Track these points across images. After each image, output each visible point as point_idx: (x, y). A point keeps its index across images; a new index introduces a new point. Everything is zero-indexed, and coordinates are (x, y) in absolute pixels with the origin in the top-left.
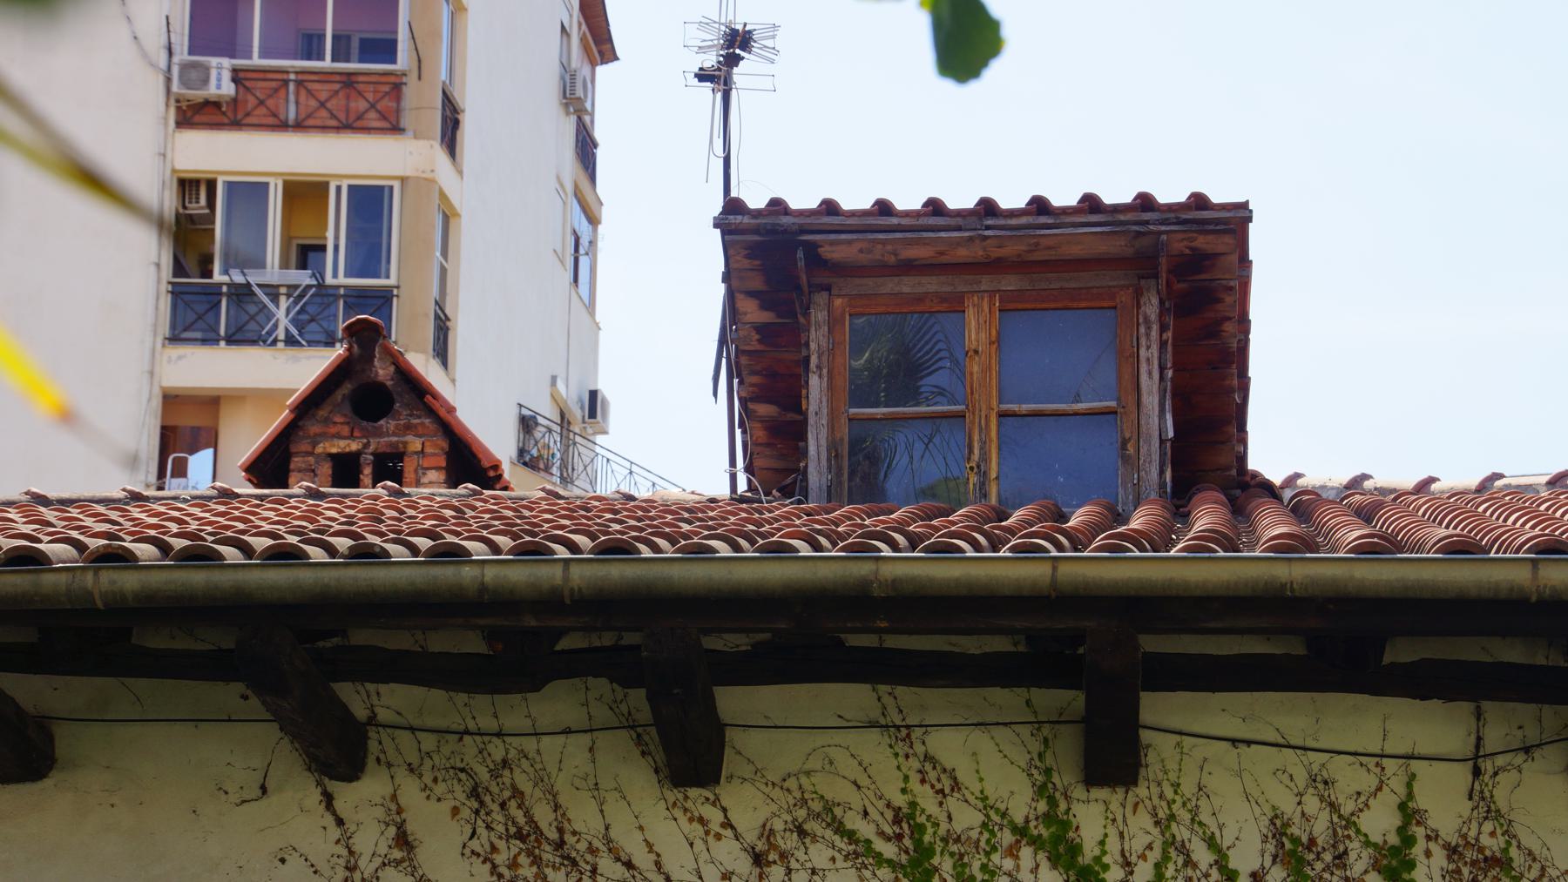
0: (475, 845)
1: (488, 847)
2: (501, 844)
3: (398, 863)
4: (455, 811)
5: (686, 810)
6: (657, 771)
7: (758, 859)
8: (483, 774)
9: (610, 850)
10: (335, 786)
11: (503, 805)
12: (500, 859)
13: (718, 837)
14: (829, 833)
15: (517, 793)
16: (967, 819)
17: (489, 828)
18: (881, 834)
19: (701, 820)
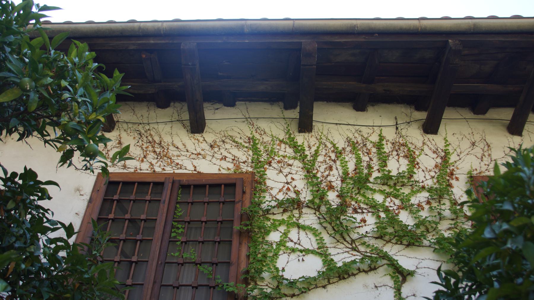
0: (138, 144)
1: (141, 145)
2: (145, 144)
3: (117, 147)
4: (134, 138)
5: (194, 138)
6: (187, 131)
7: (212, 146)
8: (143, 132)
9: (173, 145)
11: (147, 137)
12: (143, 147)
13: (202, 143)
14: (231, 142)
15: (151, 135)
16: (267, 139)
17: (142, 141)
18: (245, 142)
19: (197, 140)
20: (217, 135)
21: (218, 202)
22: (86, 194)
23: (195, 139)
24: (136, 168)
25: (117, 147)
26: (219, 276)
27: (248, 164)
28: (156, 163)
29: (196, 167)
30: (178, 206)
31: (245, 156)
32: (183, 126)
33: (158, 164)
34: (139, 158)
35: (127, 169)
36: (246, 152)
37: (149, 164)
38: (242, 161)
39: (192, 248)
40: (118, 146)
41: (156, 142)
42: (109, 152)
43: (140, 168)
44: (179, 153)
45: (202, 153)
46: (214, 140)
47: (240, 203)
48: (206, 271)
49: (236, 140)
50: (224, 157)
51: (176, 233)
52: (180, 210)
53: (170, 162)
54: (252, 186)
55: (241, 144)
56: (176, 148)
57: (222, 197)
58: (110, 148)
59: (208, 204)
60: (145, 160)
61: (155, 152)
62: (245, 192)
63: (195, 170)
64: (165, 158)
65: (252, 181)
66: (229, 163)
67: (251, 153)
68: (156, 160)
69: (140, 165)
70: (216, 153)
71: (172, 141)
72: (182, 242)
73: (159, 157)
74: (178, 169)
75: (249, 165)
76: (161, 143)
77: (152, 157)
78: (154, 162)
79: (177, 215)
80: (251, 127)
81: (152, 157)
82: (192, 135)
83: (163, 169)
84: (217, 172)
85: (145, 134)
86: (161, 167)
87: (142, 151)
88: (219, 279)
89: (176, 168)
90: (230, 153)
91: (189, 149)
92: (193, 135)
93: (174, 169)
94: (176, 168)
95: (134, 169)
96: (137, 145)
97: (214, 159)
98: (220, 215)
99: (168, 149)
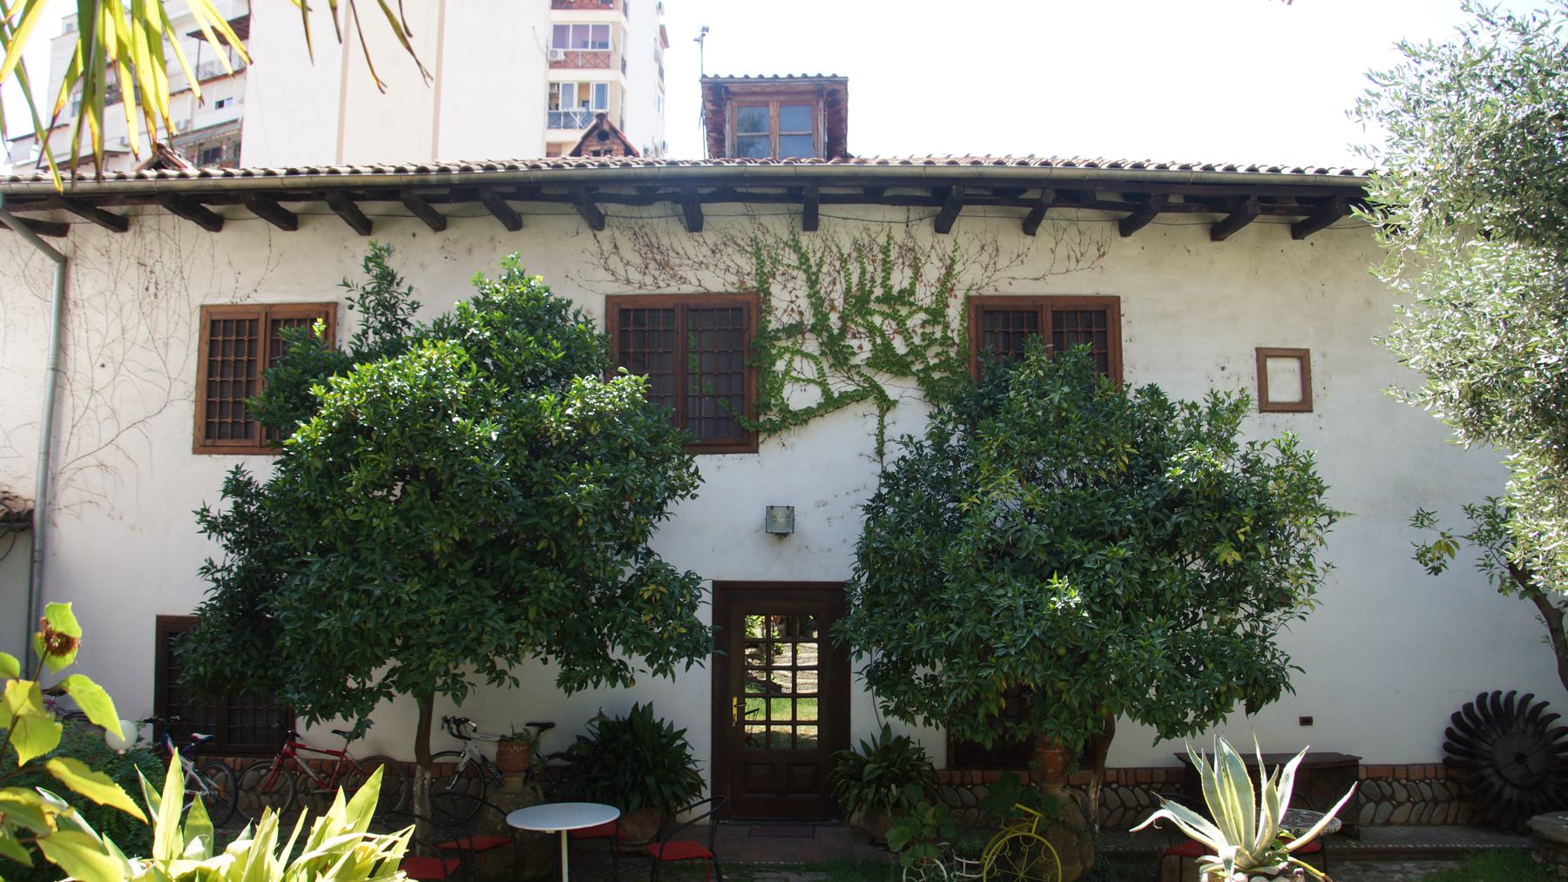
7: (713, 252)
10: (597, 232)
16: (771, 240)
45: (705, 261)
61: (655, 260)
67: (754, 261)
78: (657, 274)
84: (722, 290)
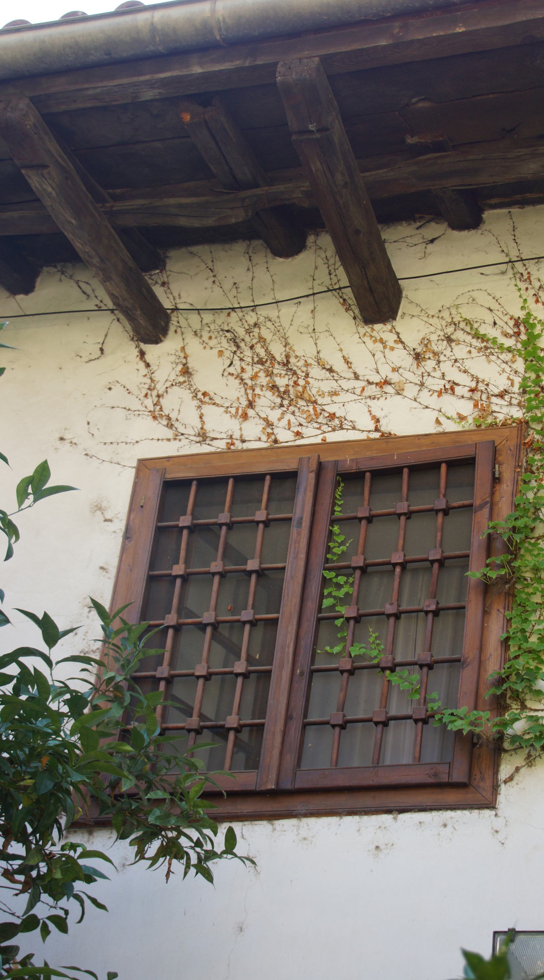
0: (231, 370)
1: (239, 371)
2: (248, 368)
3: (181, 383)
4: (221, 353)
5: (371, 336)
6: (355, 318)
7: (418, 357)
8: (241, 332)
9: (318, 363)
10: (145, 347)
11: (252, 347)
12: (246, 376)
13: (392, 349)
14: (469, 338)
15: (262, 339)
17: (241, 360)
18: (506, 335)
19: (381, 341)
20: (431, 321)
21: (431, 510)
22: (118, 518)
23: (375, 341)
24: (231, 437)
25: (181, 383)
26: (435, 695)
27: (511, 397)
28: (279, 420)
29: (378, 421)
30: (336, 529)
31: (505, 375)
32: (342, 305)
33: (284, 422)
34: (237, 409)
35: (210, 443)
36: (506, 363)
37: (262, 422)
38: (496, 392)
39: (374, 632)
40: (181, 379)
41: (275, 360)
42: (161, 399)
43: (241, 436)
44: (334, 384)
45: (394, 377)
46: (423, 339)
47: (486, 510)
48: (406, 683)
49: (482, 331)
50: (451, 384)
51: (335, 598)
52: (340, 539)
53: (312, 412)
54: (518, 459)
55: (494, 340)
56: (328, 370)
57: (441, 496)
58: (163, 389)
59: (408, 518)
60: (251, 412)
61: (274, 387)
62: (498, 479)
63: (377, 430)
64: (301, 403)
65: (518, 448)
66: (462, 400)
67: (520, 365)
68: (280, 411)
69: (241, 429)
70: (429, 375)
71: (316, 354)
72: (348, 619)
73: (286, 402)
74: (334, 430)
75: (515, 402)
76: (288, 362)
77: (269, 403)
78: (274, 415)
79: (334, 554)
80: (523, 285)
81: (269, 403)
82: (367, 329)
83: (298, 434)
84: (432, 429)
85: (247, 339)
86: (292, 429)
87: (243, 390)
88: (434, 701)
89: (330, 429)
90: (465, 372)
91: (360, 372)
92: (369, 330)
93: (325, 432)
94: (330, 429)
95: (225, 441)
96: (229, 374)
97: (425, 393)
98: (438, 545)
99: (307, 375)
